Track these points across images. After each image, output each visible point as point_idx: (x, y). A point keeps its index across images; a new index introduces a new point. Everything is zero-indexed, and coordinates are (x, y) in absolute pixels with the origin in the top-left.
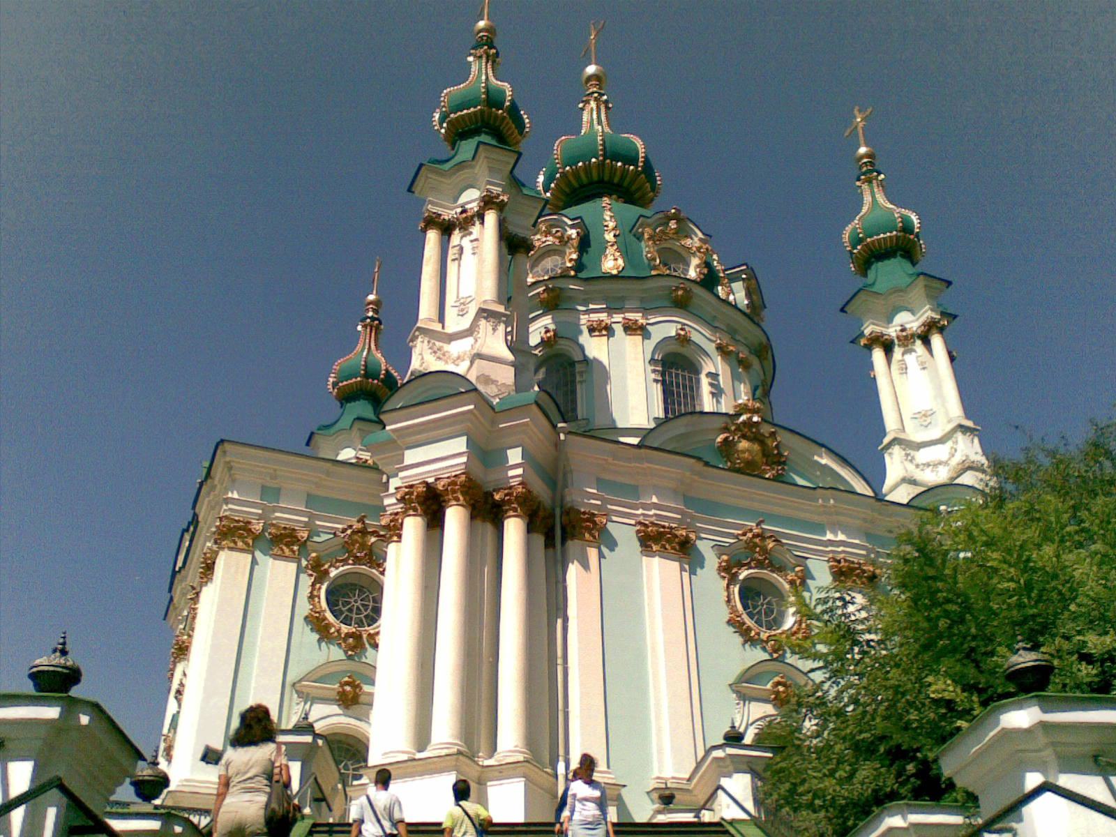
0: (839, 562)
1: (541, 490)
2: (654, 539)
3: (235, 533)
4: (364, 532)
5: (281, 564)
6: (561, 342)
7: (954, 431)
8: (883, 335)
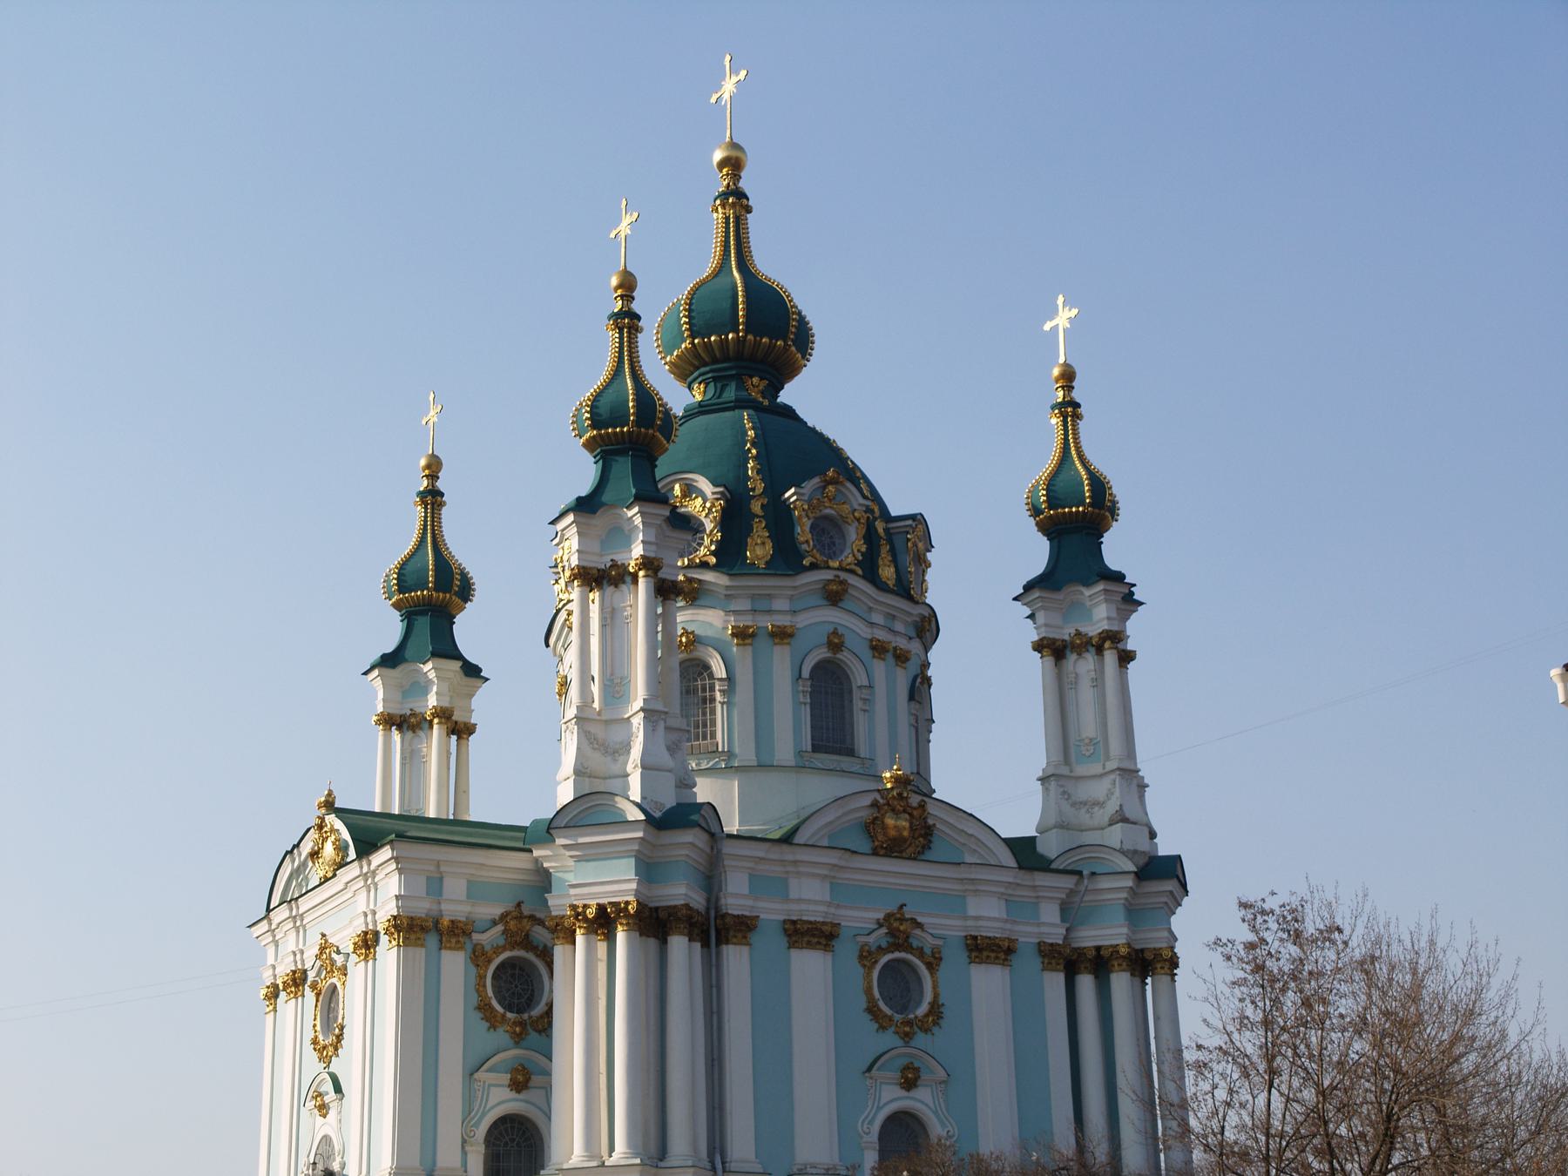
0: (975, 938)
1: (698, 900)
3: (409, 928)
4: (520, 917)
5: (446, 954)
6: (701, 648)
7: (1112, 771)
8: (1054, 641)
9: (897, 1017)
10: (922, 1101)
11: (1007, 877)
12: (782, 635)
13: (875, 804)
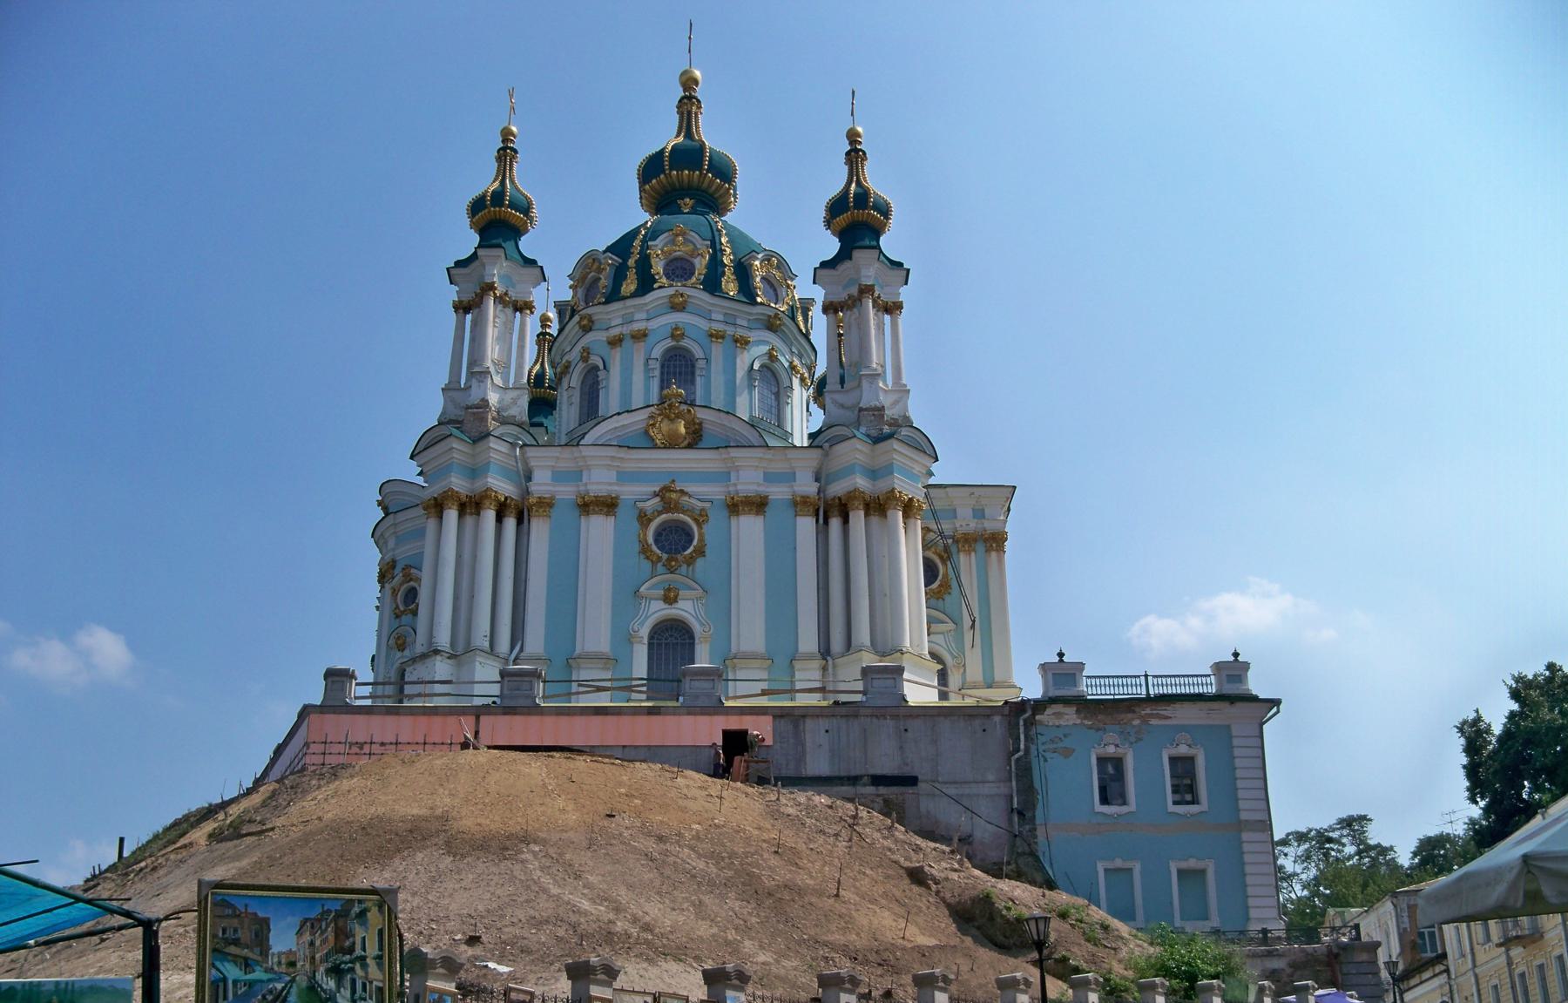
2: (587, 506)
9: (665, 556)
10: (685, 609)
11: (758, 453)
12: (640, 336)
13: (651, 417)
